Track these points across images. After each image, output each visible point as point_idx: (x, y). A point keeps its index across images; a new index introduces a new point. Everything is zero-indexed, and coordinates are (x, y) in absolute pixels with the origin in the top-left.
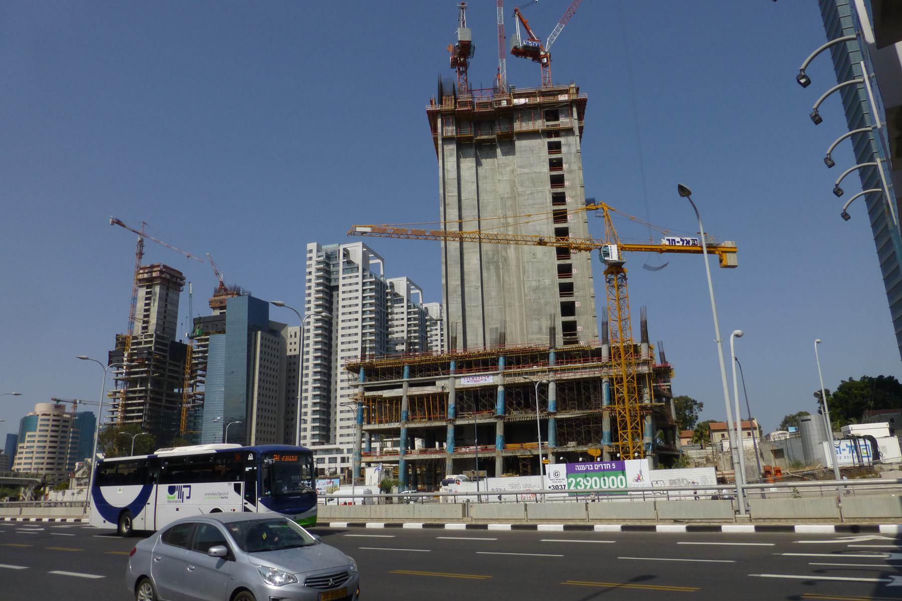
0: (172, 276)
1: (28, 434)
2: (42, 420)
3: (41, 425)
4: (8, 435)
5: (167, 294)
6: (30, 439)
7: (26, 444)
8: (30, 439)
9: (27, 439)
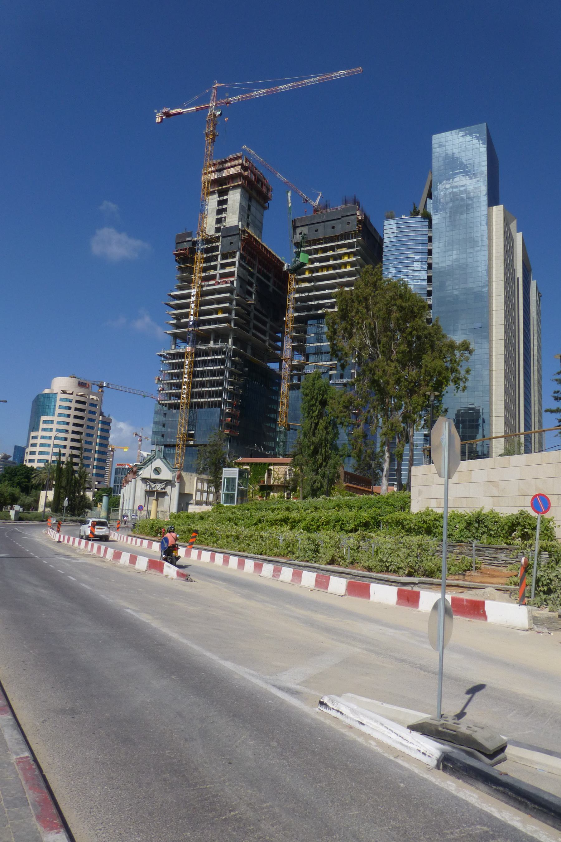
0: (258, 180)
1: (43, 418)
2: (62, 400)
3: (60, 407)
4: (16, 447)
6: (45, 426)
7: (40, 433)
8: (45, 426)
9: (42, 426)
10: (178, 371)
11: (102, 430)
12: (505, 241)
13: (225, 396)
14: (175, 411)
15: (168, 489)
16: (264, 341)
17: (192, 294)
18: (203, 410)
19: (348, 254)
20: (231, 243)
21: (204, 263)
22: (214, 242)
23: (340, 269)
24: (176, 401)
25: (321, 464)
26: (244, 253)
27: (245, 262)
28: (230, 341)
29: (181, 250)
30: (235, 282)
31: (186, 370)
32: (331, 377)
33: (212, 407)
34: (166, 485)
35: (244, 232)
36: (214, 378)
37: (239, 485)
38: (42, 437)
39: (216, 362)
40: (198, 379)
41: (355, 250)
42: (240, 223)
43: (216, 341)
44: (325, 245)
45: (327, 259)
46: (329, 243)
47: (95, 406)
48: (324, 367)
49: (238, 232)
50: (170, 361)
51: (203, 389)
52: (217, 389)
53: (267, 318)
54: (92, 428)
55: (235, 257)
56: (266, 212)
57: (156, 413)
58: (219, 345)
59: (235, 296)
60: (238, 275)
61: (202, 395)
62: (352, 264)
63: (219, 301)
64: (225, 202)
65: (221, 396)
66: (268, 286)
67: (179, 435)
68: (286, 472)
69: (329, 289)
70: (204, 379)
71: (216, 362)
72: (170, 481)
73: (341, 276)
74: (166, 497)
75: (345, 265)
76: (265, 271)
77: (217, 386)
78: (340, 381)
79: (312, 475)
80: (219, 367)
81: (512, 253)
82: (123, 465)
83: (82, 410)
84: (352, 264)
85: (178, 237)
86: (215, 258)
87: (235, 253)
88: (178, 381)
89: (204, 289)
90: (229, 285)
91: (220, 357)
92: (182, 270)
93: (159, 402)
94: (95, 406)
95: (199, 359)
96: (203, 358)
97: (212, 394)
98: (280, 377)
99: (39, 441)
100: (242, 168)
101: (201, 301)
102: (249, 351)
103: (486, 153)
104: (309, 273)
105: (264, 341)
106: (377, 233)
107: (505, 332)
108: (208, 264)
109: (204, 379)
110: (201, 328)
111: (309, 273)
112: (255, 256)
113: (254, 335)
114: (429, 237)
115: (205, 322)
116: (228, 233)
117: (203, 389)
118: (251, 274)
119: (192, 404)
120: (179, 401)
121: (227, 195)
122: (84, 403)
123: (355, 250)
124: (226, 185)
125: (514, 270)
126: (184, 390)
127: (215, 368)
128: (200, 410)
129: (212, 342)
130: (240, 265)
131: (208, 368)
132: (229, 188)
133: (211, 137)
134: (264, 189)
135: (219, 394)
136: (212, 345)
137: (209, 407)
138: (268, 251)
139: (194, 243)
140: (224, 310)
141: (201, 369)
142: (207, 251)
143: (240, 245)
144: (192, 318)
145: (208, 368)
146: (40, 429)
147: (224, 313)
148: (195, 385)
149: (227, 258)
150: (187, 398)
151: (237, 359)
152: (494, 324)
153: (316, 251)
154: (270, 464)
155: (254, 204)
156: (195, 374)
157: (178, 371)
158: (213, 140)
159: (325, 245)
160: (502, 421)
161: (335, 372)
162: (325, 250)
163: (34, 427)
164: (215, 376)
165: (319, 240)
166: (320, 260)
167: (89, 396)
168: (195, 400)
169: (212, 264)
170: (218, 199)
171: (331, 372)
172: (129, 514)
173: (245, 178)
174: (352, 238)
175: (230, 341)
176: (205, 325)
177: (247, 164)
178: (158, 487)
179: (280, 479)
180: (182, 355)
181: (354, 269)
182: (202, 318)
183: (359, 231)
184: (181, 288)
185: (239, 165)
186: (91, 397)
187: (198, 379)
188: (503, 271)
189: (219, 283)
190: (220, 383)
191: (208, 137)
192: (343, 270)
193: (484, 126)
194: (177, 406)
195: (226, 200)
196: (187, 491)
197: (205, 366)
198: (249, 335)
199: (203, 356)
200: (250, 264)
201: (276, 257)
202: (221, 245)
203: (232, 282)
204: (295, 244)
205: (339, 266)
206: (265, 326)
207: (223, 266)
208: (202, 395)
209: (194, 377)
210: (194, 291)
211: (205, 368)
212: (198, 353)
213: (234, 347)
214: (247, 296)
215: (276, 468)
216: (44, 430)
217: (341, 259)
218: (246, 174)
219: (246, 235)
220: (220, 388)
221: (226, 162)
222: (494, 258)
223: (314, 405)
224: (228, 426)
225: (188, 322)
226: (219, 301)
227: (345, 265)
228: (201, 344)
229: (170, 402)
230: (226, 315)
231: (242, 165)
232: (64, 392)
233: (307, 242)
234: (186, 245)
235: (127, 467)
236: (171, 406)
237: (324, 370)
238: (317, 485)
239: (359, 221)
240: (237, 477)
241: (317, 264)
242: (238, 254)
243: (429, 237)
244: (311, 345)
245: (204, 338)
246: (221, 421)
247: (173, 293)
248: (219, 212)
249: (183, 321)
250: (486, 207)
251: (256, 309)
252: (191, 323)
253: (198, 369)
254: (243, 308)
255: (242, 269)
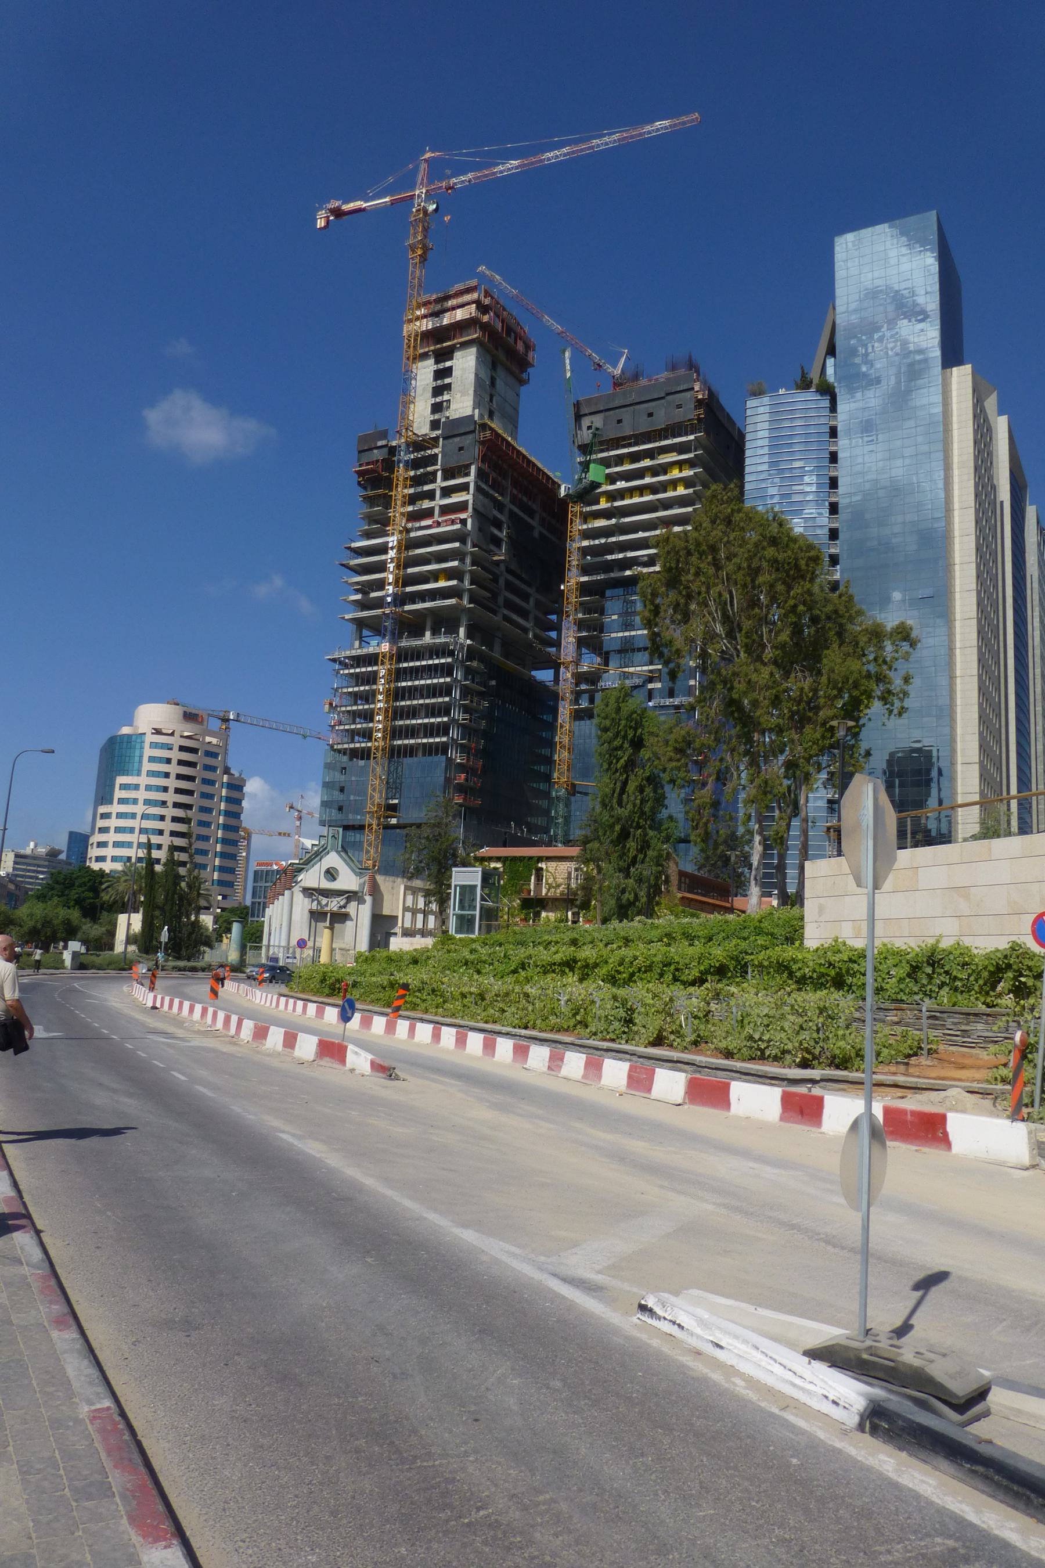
0: (509, 330)
1: (120, 780)
2: (154, 745)
3: (152, 759)
4: (71, 834)
5: (493, 383)
6: (124, 794)
7: (115, 808)
8: (124, 794)
9: (118, 794)
10: (367, 688)
11: (229, 800)
12: (975, 432)
13: (454, 733)
14: (362, 763)
15: (352, 908)
16: (525, 630)
17: (390, 545)
18: (415, 759)
19: (680, 464)
20: (461, 449)
21: (411, 486)
22: (429, 448)
23: (665, 491)
24: (363, 745)
25: (635, 857)
26: (485, 467)
27: (486, 483)
28: (462, 631)
29: (368, 464)
30: (469, 521)
31: (381, 686)
32: (650, 695)
33: (430, 754)
34: (349, 900)
35: (484, 427)
36: (433, 701)
37: (483, 899)
38: (119, 815)
39: (436, 671)
40: (403, 703)
41: (691, 455)
42: (477, 411)
43: (435, 633)
44: (636, 449)
45: (640, 474)
46: (644, 443)
47: (215, 755)
48: (638, 675)
49: (472, 428)
50: (352, 671)
51: (414, 722)
52: (439, 720)
53: (529, 585)
54: (210, 796)
55: (467, 474)
56: (523, 389)
57: (328, 766)
58: (442, 639)
59: (469, 548)
60: (474, 509)
61: (412, 732)
62: (687, 483)
63: (441, 557)
64: (448, 372)
65: (446, 733)
66: (532, 528)
67: (370, 807)
68: (570, 874)
69: (644, 531)
70: (415, 702)
71: (436, 671)
72: (355, 893)
73: (666, 505)
74: (348, 923)
75: (674, 483)
76: (525, 499)
77: (439, 716)
78: (668, 702)
79: (618, 879)
80: (442, 680)
81: (990, 454)
82: (267, 865)
83: (192, 764)
84: (687, 483)
85: (363, 439)
86: (431, 478)
87: (468, 466)
88: (366, 707)
89: (412, 535)
90: (458, 526)
91: (443, 661)
92: (370, 500)
93: (332, 746)
94: (215, 755)
95: (405, 665)
96: (411, 664)
97: (430, 730)
98: (555, 697)
99: (113, 823)
100: (477, 308)
101: (407, 558)
102: (497, 647)
103: (938, 312)
104: (607, 502)
105: (525, 630)
106: (734, 424)
107: (978, 605)
108: (419, 489)
109: (415, 702)
110: (407, 608)
111: (607, 502)
112: (505, 470)
113: (506, 618)
114: (831, 530)
115: (414, 598)
116: (454, 429)
117: (414, 722)
118: (500, 506)
119: (392, 749)
120: (369, 744)
121: (451, 359)
122: (193, 751)
123: (691, 455)
124: (450, 340)
125: (994, 488)
126: (379, 724)
127: (435, 681)
128: (407, 761)
129: (428, 634)
130: (478, 488)
131: (422, 682)
132: (454, 345)
133: (420, 252)
134: (520, 346)
135: (443, 729)
136: (428, 638)
137: (424, 755)
138: (529, 462)
139: (393, 451)
140: (449, 574)
141: (410, 684)
142: (415, 464)
143: (477, 451)
144: (390, 589)
145: (422, 682)
146: (116, 801)
147: (449, 579)
148: (399, 713)
149: (453, 477)
150: (384, 738)
151: (475, 664)
152: (957, 589)
153: (620, 460)
154: (540, 859)
155: (501, 373)
156: (399, 694)
157: (367, 688)
158: (423, 258)
159: (636, 449)
160: (975, 771)
161: (659, 685)
162: (635, 457)
163: (104, 796)
164: (434, 696)
165: (624, 438)
166: (627, 476)
167: (204, 739)
168: (399, 742)
169: (426, 488)
170: (435, 367)
171: (650, 686)
172: (281, 955)
173: (485, 327)
174: (686, 434)
175: (462, 631)
176: (414, 603)
177: (487, 301)
178: (334, 905)
179: (559, 886)
180: (372, 659)
181: (691, 491)
182: (409, 589)
183: (699, 420)
184: (368, 535)
185: (473, 302)
186: (208, 739)
187: (403, 703)
188: (972, 490)
189: (439, 524)
190: (445, 710)
191: (414, 252)
192: (670, 494)
193: (933, 215)
194: (364, 754)
195: (450, 369)
196: (386, 912)
197: (416, 679)
198: (498, 618)
199: (412, 660)
200: (496, 486)
201: (544, 473)
202: (442, 452)
203: (463, 522)
204: (580, 447)
205: (663, 487)
206: (527, 601)
207: (447, 492)
208: (412, 732)
209: (396, 699)
210: (393, 540)
211: (417, 683)
212: (403, 655)
213: (469, 642)
214: (492, 547)
215: (552, 866)
216: (122, 801)
217: (665, 473)
218: (486, 318)
219: (488, 433)
220: (445, 719)
221: (447, 298)
222: (955, 466)
223: (621, 748)
224: (461, 789)
225: (382, 599)
226: (441, 557)
227: (674, 483)
228: (408, 637)
229: (352, 746)
230: (454, 582)
231: (478, 302)
232: (158, 732)
233: (601, 443)
234: (377, 455)
235: (275, 867)
236: (354, 754)
237: (637, 681)
238: (628, 896)
239: (699, 401)
240: (479, 883)
241: (621, 485)
242: (473, 469)
243: (831, 530)
244: (613, 635)
245: (413, 626)
246: (448, 780)
247: (354, 545)
248: (437, 391)
249: (373, 595)
250: (940, 368)
251: (509, 571)
252: (389, 599)
253: (404, 684)
254: (484, 568)
255: (481, 497)
